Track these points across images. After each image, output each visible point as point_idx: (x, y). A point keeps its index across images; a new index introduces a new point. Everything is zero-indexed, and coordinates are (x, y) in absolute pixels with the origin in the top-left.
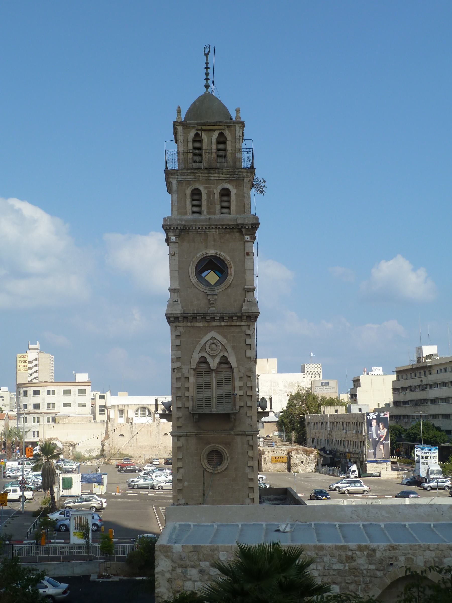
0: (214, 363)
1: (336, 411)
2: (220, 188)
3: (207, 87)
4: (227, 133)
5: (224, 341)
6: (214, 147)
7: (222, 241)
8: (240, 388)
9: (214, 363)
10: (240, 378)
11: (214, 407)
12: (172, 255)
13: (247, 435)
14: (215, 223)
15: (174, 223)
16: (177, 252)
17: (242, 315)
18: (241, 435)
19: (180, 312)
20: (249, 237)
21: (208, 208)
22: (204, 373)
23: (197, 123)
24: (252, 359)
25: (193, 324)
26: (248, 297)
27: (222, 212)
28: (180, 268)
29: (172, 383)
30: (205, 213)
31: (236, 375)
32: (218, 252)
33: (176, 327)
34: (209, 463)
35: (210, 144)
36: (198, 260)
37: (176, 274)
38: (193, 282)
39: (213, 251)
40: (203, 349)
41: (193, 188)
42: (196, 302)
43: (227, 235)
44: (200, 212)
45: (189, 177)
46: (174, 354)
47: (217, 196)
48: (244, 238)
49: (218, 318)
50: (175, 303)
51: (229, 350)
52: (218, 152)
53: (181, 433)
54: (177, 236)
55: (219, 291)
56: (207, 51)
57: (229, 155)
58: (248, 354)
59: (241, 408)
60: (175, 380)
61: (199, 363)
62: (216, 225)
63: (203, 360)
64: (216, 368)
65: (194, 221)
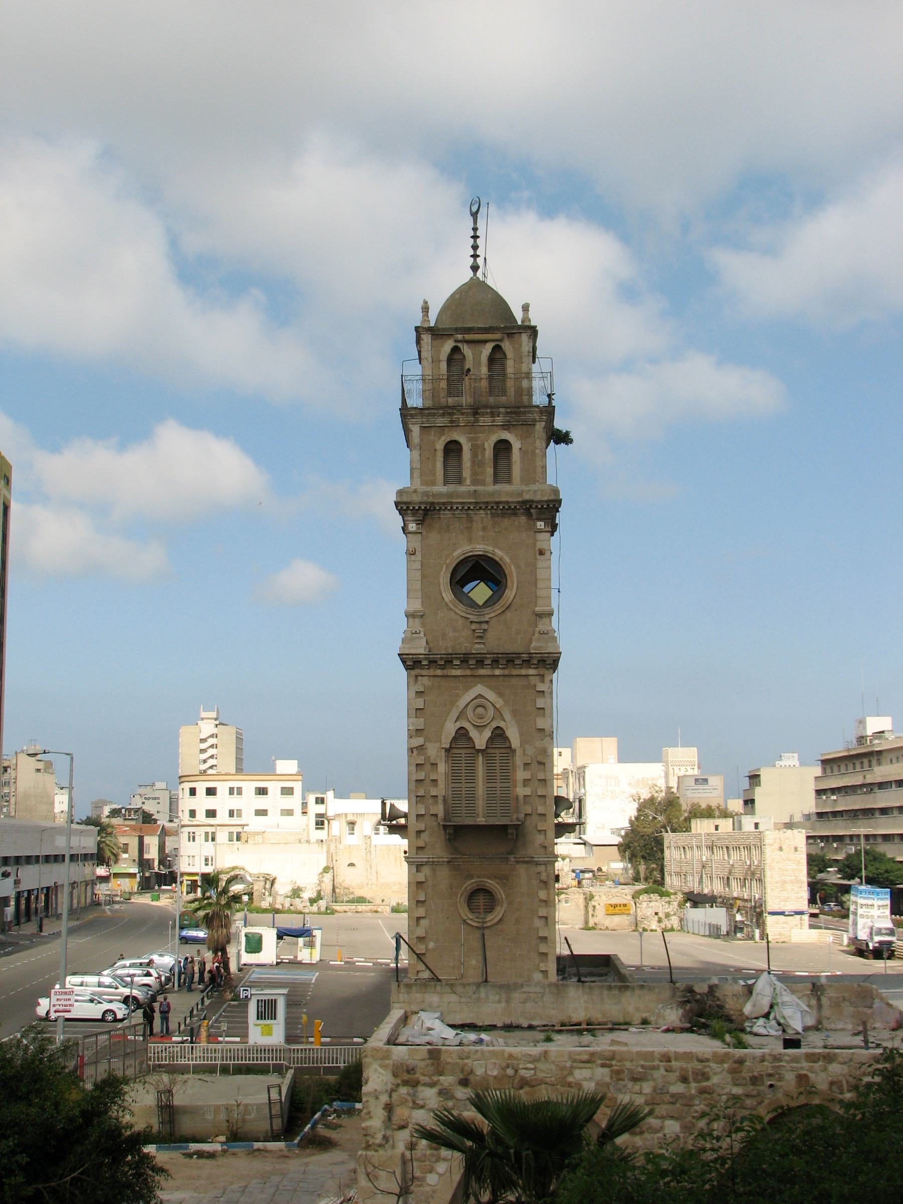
0: (480, 739)
1: (717, 828)
2: (494, 438)
3: (475, 268)
4: (506, 346)
5: (499, 702)
6: (484, 370)
7: (497, 530)
8: (526, 782)
9: (480, 739)
10: (526, 764)
11: (481, 815)
12: (411, 553)
13: (538, 864)
14: (486, 500)
15: (416, 498)
16: (419, 550)
17: (531, 657)
18: (527, 862)
19: (423, 652)
20: (542, 523)
21: (474, 473)
22: (463, 755)
23: (458, 330)
24: (547, 733)
25: (445, 672)
26: (541, 627)
27: (496, 481)
28: (423, 577)
29: (409, 774)
30: (468, 482)
31: (519, 760)
32: (490, 548)
33: (416, 676)
34: (472, 910)
35: (477, 363)
36: (456, 562)
37: (418, 586)
38: (447, 600)
39: (482, 547)
40: (462, 715)
41: (449, 439)
42: (451, 635)
43: (506, 520)
44: (460, 481)
45: (441, 421)
46: (413, 724)
47: (489, 453)
48: (535, 525)
49: (489, 662)
50: (415, 635)
51: (507, 716)
52: (490, 378)
53: (423, 857)
54: (420, 523)
55: (492, 615)
56: (474, 209)
57: (510, 383)
58: (541, 723)
59: (528, 817)
60: (414, 768)
61: (455, 739)
62: (487, 503)
63: (462, 734)
64: (484, 748)
65: (450, 495)
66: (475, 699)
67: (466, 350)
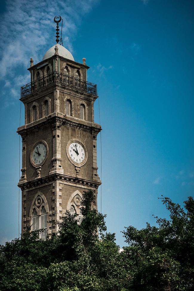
40: (73, 201)
56: (57, 20)
66: (76, 195)
67: (69, 68)
